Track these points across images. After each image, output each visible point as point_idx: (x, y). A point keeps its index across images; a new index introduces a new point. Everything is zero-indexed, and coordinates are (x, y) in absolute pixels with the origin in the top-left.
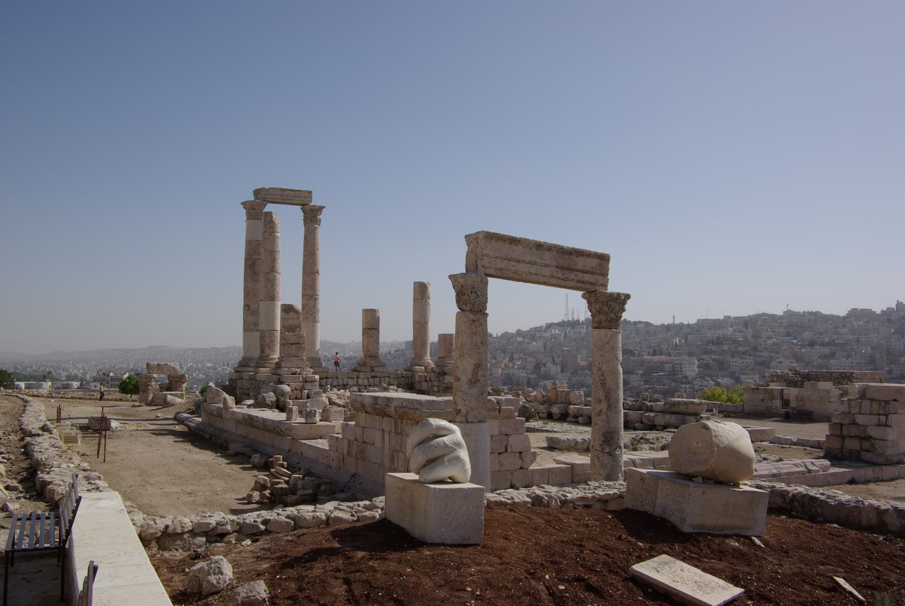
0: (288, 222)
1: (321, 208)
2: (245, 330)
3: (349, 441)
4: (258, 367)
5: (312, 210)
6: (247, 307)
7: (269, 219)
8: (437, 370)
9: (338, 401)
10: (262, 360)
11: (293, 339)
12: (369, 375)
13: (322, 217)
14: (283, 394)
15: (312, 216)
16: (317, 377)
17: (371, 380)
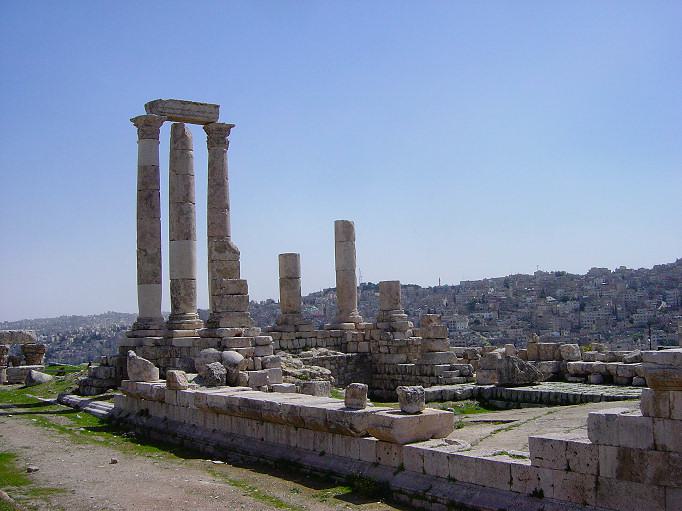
1: (227, 129)
2: (138, 284)
3: (624, 455)
4: (171, 329)
5: (220, 129)
7: (180, 133)
10: (177, 318)
11: (232, 289)
12: (293, 335)
13: (232, 137)
14: (235, 365)
15: (218, 137)
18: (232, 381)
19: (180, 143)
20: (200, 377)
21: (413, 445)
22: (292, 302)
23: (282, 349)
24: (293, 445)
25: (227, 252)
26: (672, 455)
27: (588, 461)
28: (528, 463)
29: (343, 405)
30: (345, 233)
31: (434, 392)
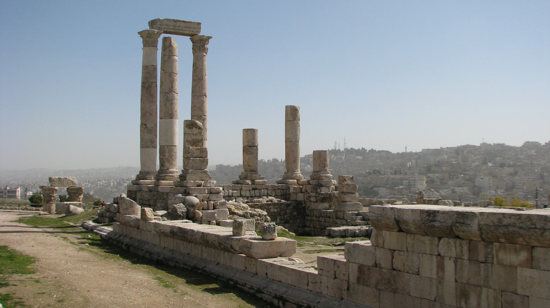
0: (182, 46)
3: (361, 268)
5: (201, 40)
6: (144, 126)
7: (168, 43)
8: (314, 182)
9: (236, 211)
10: (162, 174)
14: (193, 206)
15: (200, 45)
16: (221, 189)
17: (253, 192)
18: (191, 216)
19: (168, 47)
20: (168, 213)
21: (263, 260)
22: (250, 164)
23: (241, 196)
24: (204, 258)
25: (194, 128)
26: (383, 270)
27: (344, 272)
28: (316, 272)
29: (232, 233)
30: (292, 115)
31: (340, 230)
